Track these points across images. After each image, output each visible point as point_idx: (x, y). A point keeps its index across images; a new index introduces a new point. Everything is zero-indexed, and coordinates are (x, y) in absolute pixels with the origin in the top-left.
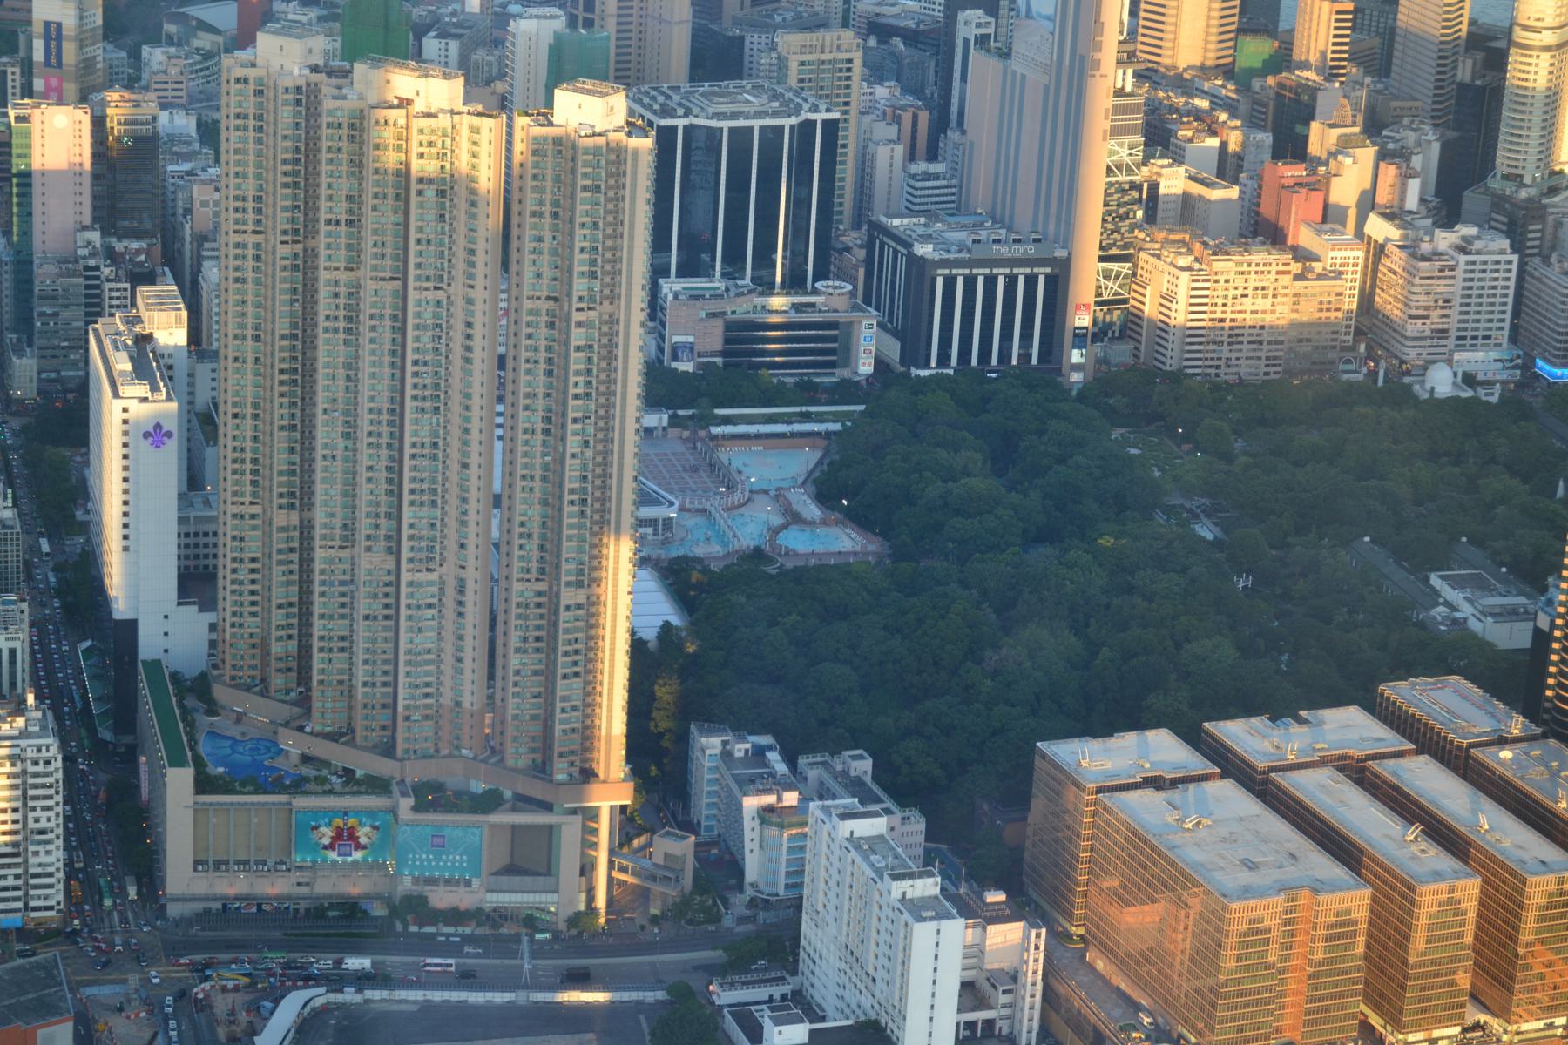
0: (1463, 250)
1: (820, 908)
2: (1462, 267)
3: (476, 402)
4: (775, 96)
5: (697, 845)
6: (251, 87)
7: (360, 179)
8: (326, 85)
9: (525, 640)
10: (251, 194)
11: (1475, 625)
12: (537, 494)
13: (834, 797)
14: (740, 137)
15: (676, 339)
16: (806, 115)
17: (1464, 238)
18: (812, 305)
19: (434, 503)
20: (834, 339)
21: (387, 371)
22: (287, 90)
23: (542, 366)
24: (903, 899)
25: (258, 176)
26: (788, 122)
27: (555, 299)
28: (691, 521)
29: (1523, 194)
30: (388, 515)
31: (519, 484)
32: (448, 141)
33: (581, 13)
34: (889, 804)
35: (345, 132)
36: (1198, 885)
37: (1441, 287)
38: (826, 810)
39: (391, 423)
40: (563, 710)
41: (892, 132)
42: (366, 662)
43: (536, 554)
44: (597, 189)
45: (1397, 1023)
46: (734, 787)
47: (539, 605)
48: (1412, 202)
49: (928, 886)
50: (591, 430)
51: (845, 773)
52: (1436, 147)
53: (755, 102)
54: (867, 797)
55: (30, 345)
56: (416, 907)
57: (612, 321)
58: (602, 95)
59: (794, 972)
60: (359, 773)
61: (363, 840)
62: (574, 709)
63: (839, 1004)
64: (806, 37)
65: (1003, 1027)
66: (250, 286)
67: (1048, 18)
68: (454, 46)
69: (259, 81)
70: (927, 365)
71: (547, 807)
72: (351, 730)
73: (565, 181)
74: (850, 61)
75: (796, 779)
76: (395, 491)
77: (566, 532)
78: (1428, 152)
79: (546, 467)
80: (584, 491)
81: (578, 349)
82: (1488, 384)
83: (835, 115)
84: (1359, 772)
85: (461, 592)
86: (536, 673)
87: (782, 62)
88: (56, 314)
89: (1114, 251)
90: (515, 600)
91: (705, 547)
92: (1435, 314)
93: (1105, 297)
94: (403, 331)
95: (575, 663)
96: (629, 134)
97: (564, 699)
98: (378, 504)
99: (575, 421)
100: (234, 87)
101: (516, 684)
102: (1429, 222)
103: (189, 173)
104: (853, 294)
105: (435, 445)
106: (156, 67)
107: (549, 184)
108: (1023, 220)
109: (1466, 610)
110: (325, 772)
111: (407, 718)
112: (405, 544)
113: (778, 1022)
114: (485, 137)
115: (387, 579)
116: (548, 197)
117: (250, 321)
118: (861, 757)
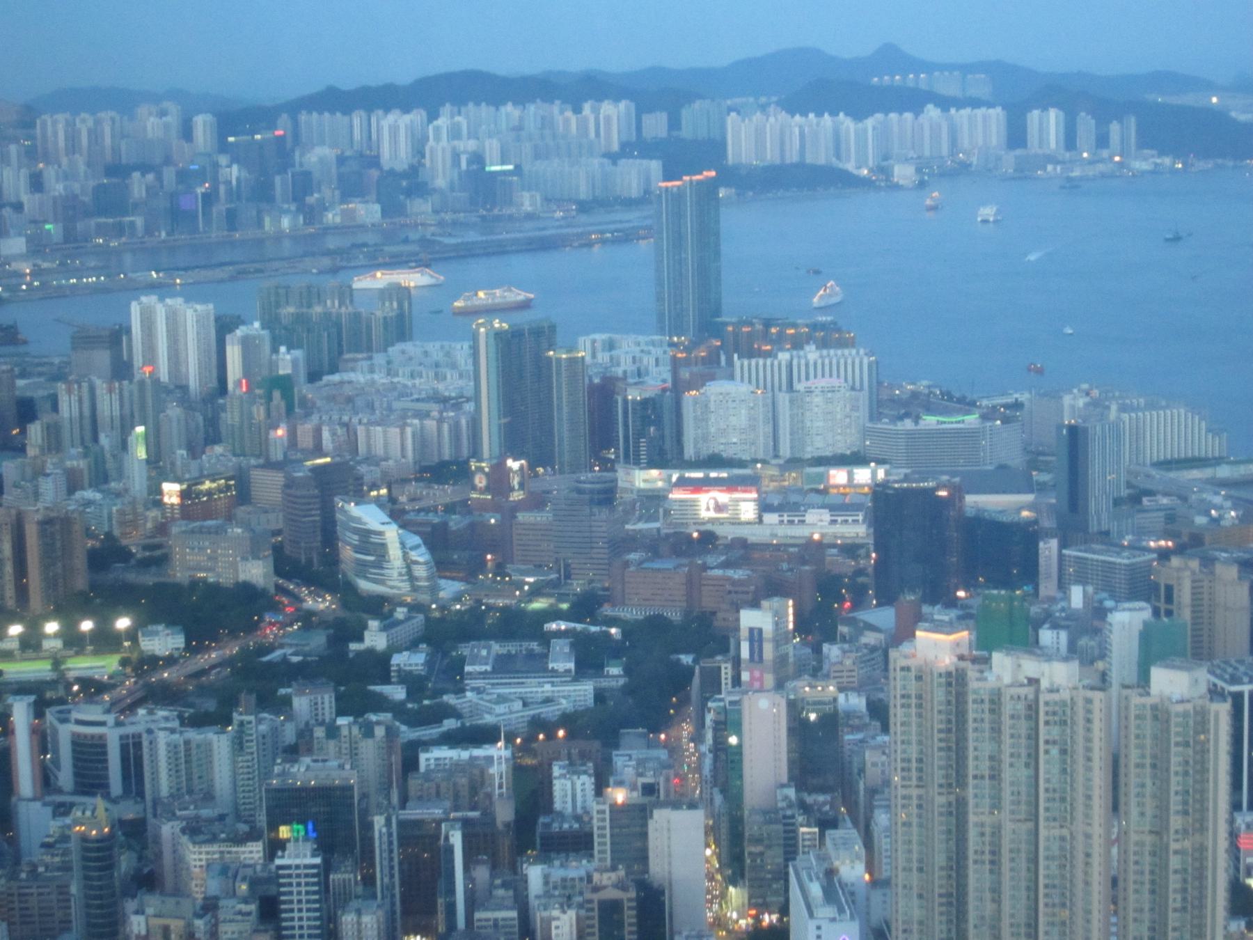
3: (1096, 917)
6: (913, 674)
7: (999, 743)
8: (972, 672)
10: (914, 756)
21: (1024, 893)
22: (940, 675)
23: (1147, 886)
25: (920, 743)
27: (1157, 833)
32: (1068, 712)
33: (1163, 606)
35: (987, 706)
44: (1187, 744)
55: (742, 876)
57: (1202, 849)
58: (1188, 669)
66: (915, 829)
69: (920, 669)
73: (1162, 739)
81: (1176, 872)
88: (762, 854)
94: (1034, 860)
96: (1211, 700)
99: (1175, 929)
100: (899, 674)
103: (862, 741)
106: (834, 660)
107: (1148, 742)
116: (1148, 752)
117: (915, 856)
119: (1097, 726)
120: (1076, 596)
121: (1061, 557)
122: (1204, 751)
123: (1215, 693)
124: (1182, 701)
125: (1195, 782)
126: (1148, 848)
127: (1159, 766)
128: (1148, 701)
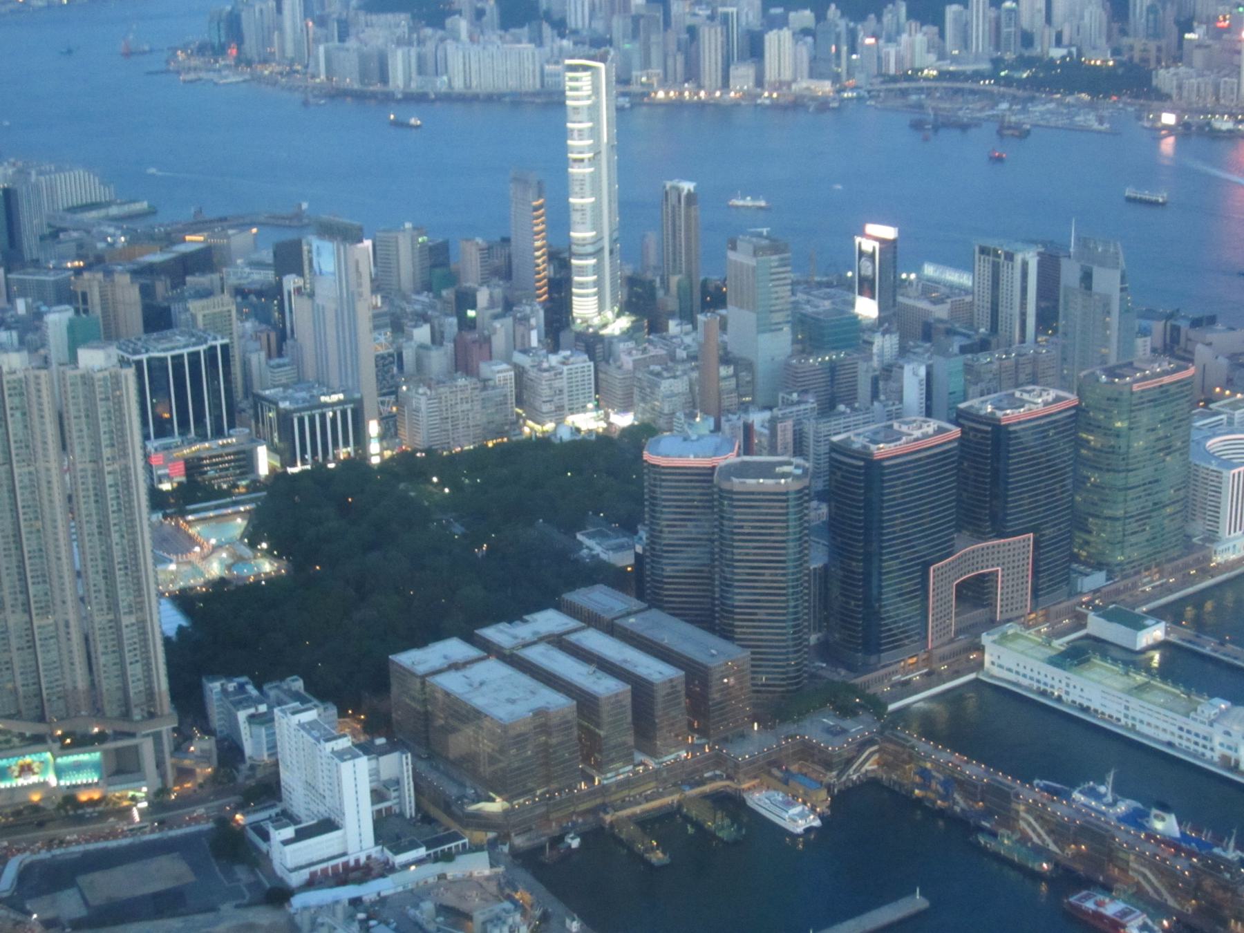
0: (563, 363)
1: (289, 763)
2: (565, 372)
3: (60, 523)
4: (193, 335)
5: (217, 742)
9: (106, 647)
11: (604, 556)
12: (100, 568)
13: (286, 703)
14: (178, 360)
15: (160, 472)
16: (211, 343)
17: (565, 357)
18: (228, 445)
19: (45, 582)
20: (244, 459)
23: (92, 498)
24: (333, 752)
26: (202, 348)
27: (94, 462)
28: (185, 568)
29: (591, 330)
30: (21, 592)
31: (89, 564)
32: (24, 385)
33: (81, 307)
34: (316, 702)
36: (486, 716)
37: (557, 384)
38: (283, 711)
39: (14, 542)
40: (133, 682)
41: (257, 345)
42: (22, 673)
43: (104, 599)
44: (107, 399)
45: (600, 767)
46: (231, 707)
47: (111, 627)
48: (534, 342)
49: (345, 743)
50: (124, 529)
51: (290, 690)
52: (542, 313)
53: (182, 340)
54: (303, 700)
56: (69, 799)
57: (126, 469)
58: (102, 348)
59: (280, 800)
60: (28, 734)
61: (36, 770)
62: (139, 680)
63: (307, 812)
64: (204, 302)
65: (396, 809)
67: (334, 274)
68: (15, 334)
70: (294, 464)
71: (132, 735)
72: (19, 712)
73: (90, 399)
74: (229, 311)
75: (263, 697)
76: (23, 578)
77: (119, 586)
78: (538, 318)
79: (102, 553)
80: (125, 562)
81: (111, 486)
82: (590, 432)
83: (226, 341)
84: (559, 642)
85: (67, 625)
86: (115, 664)
87: (194, 317)
89: (385, 391)
90: (97, 626)
91: (197, 582)
92: (556, 398)
93: (384, 415)
94: (13, 491)
95: (136, 655)
96: (121, 367)
97: (132, 675)
98: (15, 587)
99: (115, 525)
101: (105, 672)
102: (544, 351)
104: (250, 434)
105: (41, 550)
107: (81, 400)
108: (335, 382)
109: (598, 550)
110: (9, 736)
111: (49, 700)
112: (33, 606)
113: (277, 828)
114: (43, 380)
115: (26, 627)
118: (296, 680)
119: (44, 393)
120: (21, 306)
121: (7, 280)
122: (120, 403)
123: (123, 362)
124: (100, 371)
125: (116, 424)
126: (90, 473)
127: (91, 415)
128: (78, 372)
